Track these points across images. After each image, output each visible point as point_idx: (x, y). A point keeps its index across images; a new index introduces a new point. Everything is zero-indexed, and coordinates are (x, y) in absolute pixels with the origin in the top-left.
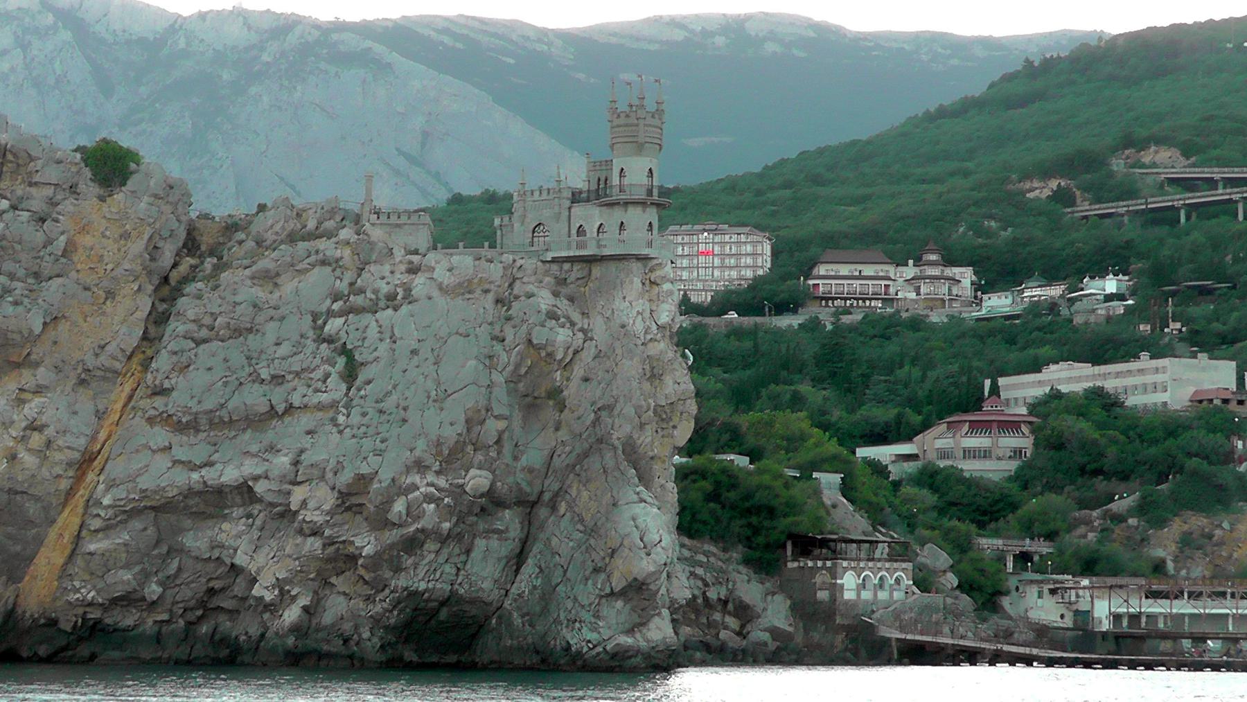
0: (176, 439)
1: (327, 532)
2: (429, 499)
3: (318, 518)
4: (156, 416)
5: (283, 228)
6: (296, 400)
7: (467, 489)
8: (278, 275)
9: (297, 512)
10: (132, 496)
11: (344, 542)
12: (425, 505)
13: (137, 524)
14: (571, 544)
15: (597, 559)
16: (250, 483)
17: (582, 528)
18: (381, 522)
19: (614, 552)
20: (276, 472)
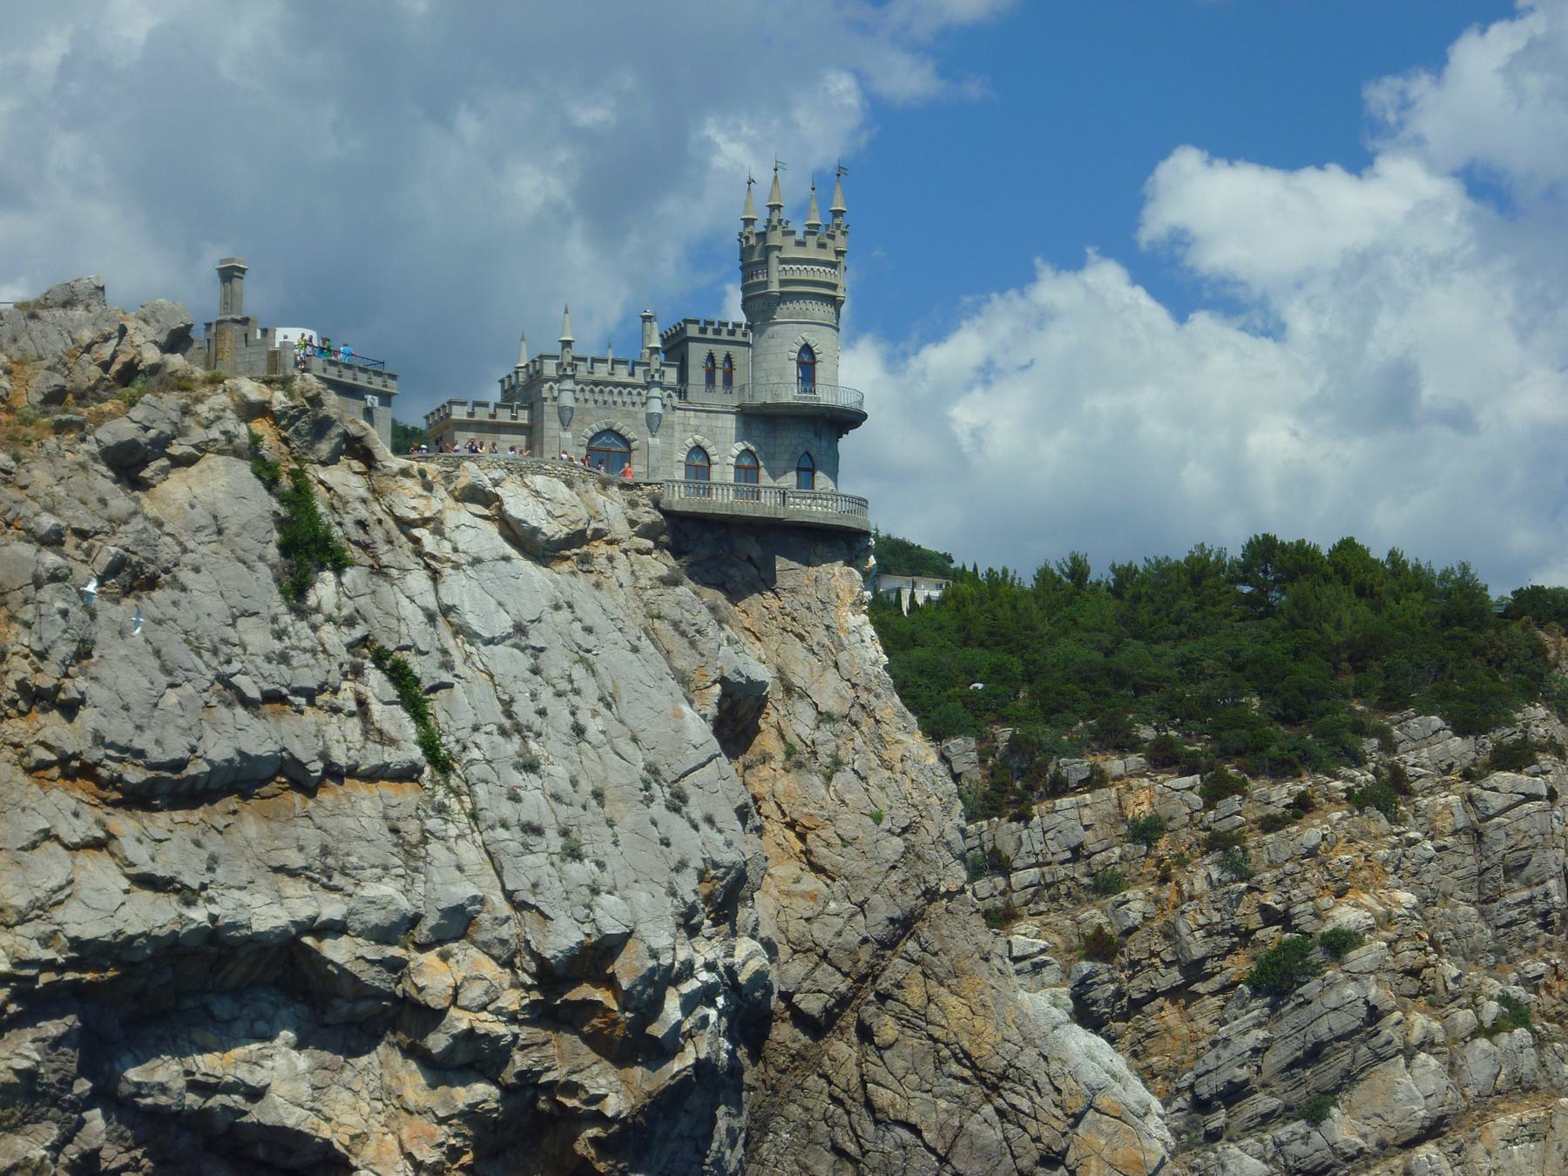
0: (125, 825)
1: (520, 1061)
2: (706, 995)
3: (500, 1029)
4: (46, 765)
5: (114, 357)
6: (340, 757)
7: (743, 978)
8: (145, 464)
9: (442, 1013)
10: (48, 954)
11: (552, 1084)
12: (702, 1011)
13: (53, 1028)
14: (943, 1104)
15: (1047, 1134)
16: (308, 940)
17: (967, 1073)
18: (634, 1045)
19: (1078, 1118)
20: (374, 917)
